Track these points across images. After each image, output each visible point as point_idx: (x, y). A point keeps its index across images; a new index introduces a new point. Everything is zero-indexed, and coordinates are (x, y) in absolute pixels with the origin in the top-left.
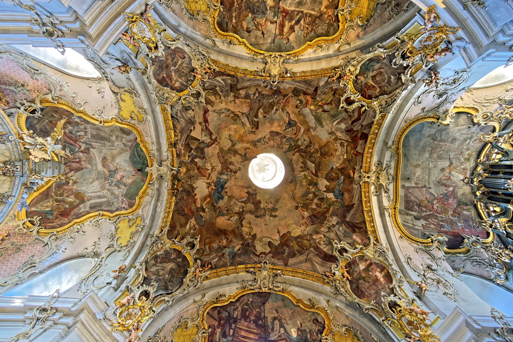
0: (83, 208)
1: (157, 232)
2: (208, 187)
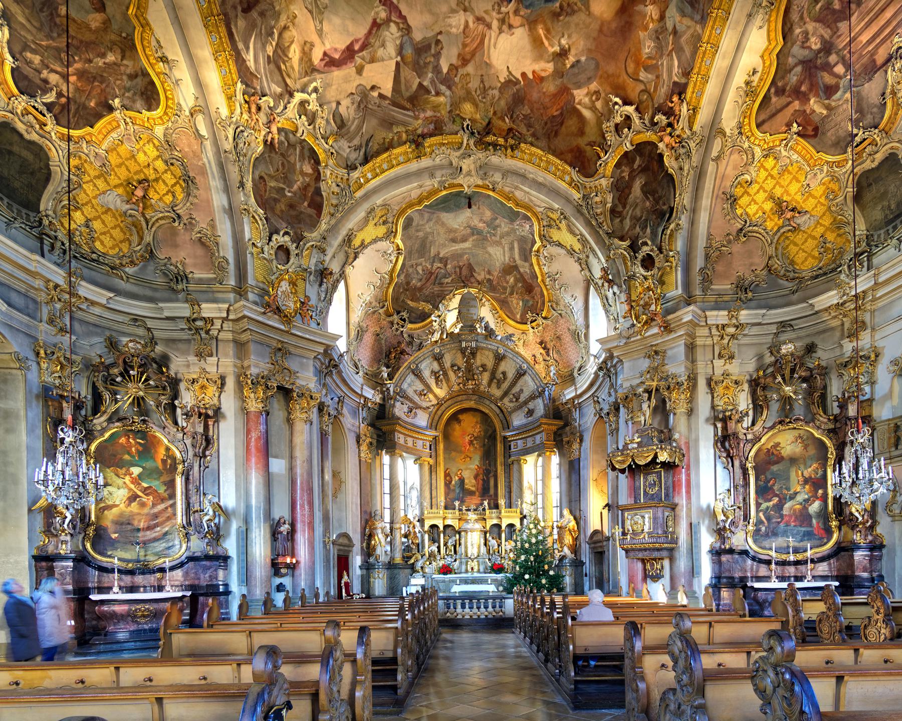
0: (524, 268)
1: (576, 195)
2: (510, 27)
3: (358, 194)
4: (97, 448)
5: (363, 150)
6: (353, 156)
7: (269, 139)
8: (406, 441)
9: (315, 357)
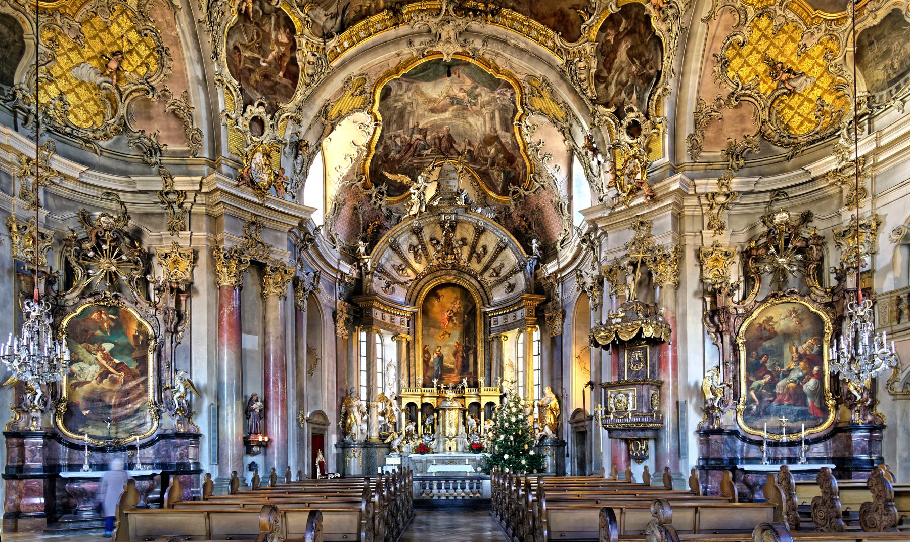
0: (506, 138)
3: (334, 64)
4: (69, 324)
5: (340, 18)
6: (329, 24)
7: (244, 8)
8: (383, 317)
9: (290, 231)
